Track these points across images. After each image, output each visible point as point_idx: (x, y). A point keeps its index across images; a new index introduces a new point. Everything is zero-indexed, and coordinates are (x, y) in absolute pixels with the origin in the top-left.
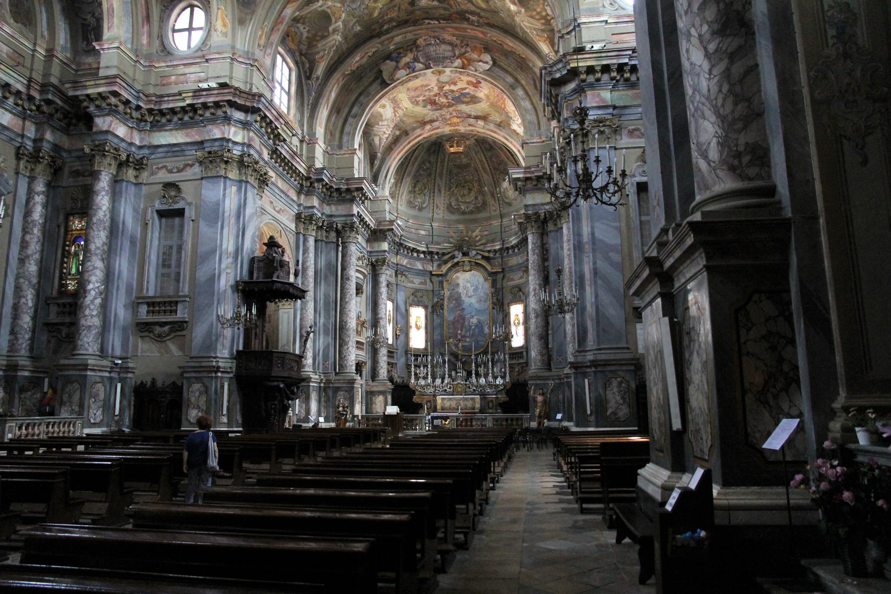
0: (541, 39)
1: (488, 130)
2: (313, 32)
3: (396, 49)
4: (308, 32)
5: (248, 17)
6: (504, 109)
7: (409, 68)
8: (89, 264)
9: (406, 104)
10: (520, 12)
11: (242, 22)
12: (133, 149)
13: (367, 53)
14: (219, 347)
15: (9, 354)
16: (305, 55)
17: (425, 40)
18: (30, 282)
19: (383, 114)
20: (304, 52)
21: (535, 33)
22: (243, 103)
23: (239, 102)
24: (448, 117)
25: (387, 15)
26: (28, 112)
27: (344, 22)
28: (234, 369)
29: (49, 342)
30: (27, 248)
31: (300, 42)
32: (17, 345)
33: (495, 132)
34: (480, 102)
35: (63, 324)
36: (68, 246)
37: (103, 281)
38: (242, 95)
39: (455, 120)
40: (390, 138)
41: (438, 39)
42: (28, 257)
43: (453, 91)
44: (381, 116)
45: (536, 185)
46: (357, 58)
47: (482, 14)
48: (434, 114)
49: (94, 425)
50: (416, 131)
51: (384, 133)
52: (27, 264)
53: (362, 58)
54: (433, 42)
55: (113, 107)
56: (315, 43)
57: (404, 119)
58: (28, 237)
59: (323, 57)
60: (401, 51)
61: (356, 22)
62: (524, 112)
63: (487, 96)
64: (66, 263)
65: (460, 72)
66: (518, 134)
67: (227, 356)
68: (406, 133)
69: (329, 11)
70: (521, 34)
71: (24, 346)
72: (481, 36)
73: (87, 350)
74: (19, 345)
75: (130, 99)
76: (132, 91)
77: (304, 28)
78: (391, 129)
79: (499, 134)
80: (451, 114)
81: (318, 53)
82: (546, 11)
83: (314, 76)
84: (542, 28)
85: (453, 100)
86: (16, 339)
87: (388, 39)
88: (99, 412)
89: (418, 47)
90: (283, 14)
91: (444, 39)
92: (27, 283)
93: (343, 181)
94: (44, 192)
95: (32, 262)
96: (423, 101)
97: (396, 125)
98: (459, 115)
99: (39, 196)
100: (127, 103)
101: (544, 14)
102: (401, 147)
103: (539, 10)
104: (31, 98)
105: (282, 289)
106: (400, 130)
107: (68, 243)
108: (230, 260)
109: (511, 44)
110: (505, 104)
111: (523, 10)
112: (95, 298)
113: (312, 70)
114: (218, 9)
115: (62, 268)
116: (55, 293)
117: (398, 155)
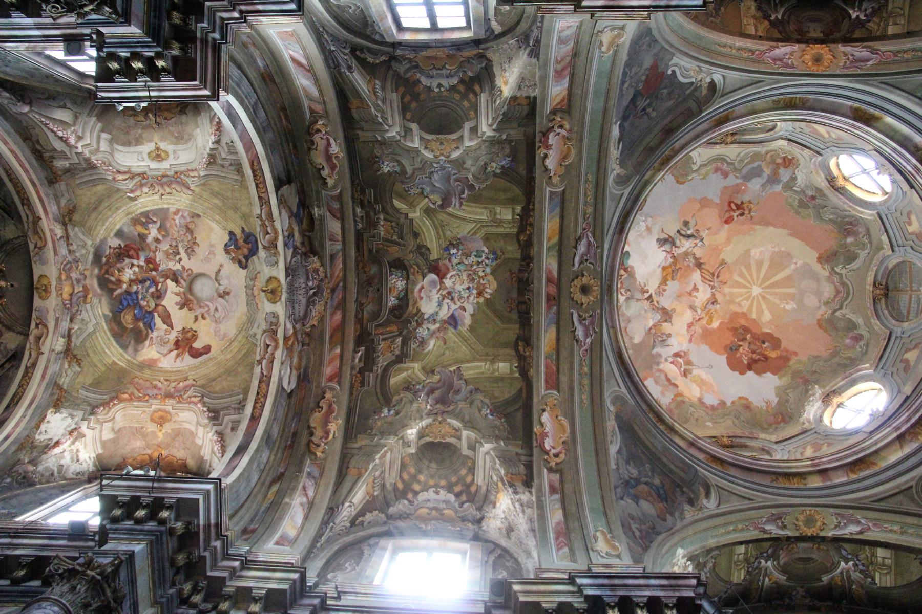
0: (370, 485)
1: (48, 360)
2: (422, 97)
3: (311, 219)
4: (429, 89)
6: (117, 397)
7: (288, 237)
9: (148, 201)
10: (407, 444)
13: (333, 168)
16: (387, 64)
17: (316, 271)
19: (140, 148)
20: (393, 64)
21: (377, 473)
24: (74, 275)
25: (385, 219)
27: (417, 151)
31: (417, 67)
33: (43, 377)
34: (124, 347)
39: (67, 289)
40: (58, 146)
41: (314, 294)
43: (159, 296)
44: (127, 144)
45: (172, 563)
46: (335, 149)
47: (371, 378)
48: (84, 245)
50: (53, 202)
51: (80, 138)
53: (328, 157)
54: (310, 284)
56: (402, 89)
57: (100, 188)
59: (375, 93)
60: (305, 226)
61: (404, 172)
62: (246, 474)
63: (150, 365)
65: (275, 332)
66: (38, 426)
68: (52, 179)
69: (453, 136)
70: (356, 446)
72: (328, 371)
77: (440, 86)
78: (87, 155)
79: (39, 385)
80: (78, 281)
81: (383, 88)
82: (426, 490)
83: (354, 63)
84: (388, 486)
85: (128, 292)
87: (342, 210)
89: (305, 255)
90: (566, 82)
91: (314, 305)
93: (217, 35)
96: (142, 237)
97: (92, 167)
98: (75, 299)
101: (416, 487)
102: (27, 165)
103: (422, 478)
106: (67, 171)
109: (332, 427)
110: (131, 400)
111: (412, 450)
113: (362, 62)
117: (12, 152)
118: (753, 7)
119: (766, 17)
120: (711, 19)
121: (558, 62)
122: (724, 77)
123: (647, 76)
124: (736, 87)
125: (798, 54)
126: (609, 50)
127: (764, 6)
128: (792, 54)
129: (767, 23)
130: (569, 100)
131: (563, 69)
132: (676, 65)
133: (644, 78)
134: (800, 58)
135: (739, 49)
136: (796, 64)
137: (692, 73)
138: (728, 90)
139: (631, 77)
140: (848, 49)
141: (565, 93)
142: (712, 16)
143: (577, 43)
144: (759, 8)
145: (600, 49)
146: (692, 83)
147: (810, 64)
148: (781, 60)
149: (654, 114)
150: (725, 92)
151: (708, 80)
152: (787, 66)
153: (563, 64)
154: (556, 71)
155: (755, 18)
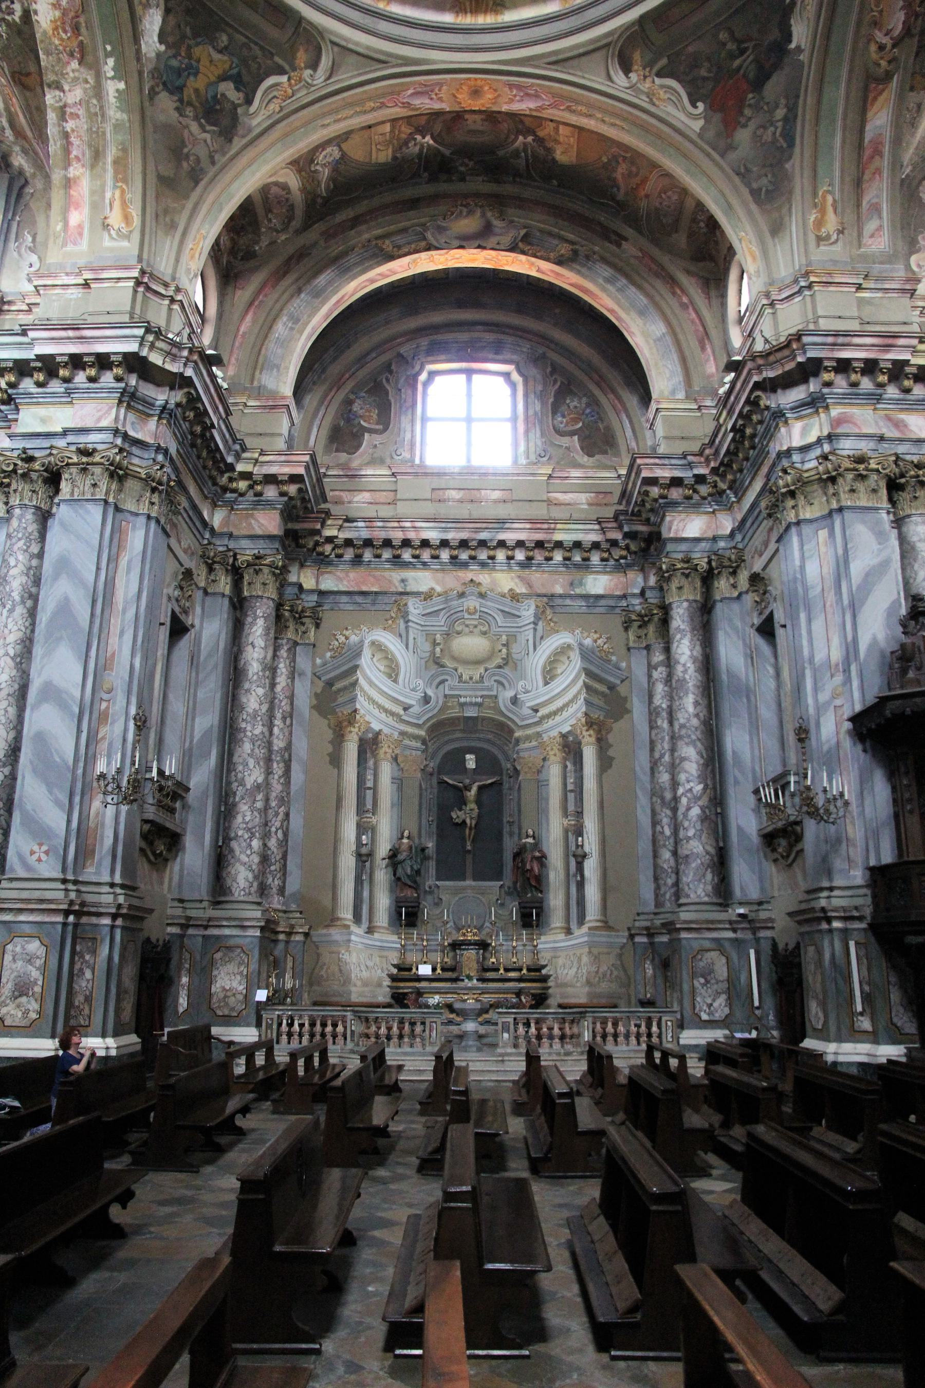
5: (784, 211)
11: (777, 229)
12: (722, 544)
14: (838, 864)
22: (780, 372)
23: (771, 374)
26: (622, 561)
28: (868, 912)
37: (699, 776)
38: (772, 358)
49: (711, 1024)
55: (661, 501)
67: (859, 881)
73: (688, 896)
75: (677, 474)
76: (673, 462)
88: (721, 1001)
90: (869, 134)
100: (676, 482)
104: (614, 543)
105: (908, 711)
108: (839, 678)
112: (689, 809)
114: (740, 240)
118: (558, 152)
119: (540, 141)
120: (628, 155)
121: (878, 171)
122: (609, 78)
123: (741, 113)
124: (584, 59)
125: (500, 100)
126: (824, 197)
127: (542, 151)
128: (511, 101)
129: (541, 134)
130: (865, 100)
131: (872, 157)
132: (695, 117)
133: (747, 112)
134: (499, 96)
135: (590, 116)
136: (507, 89)
137: (662, 94)
138: (599, 55)
139: (772, 123)
140: (437, 106)
141: (870, 114)
142: (625, 158)
143: (858, 205)
144: (549, 151)
145: (834, 200)
146: (659, 75)
147: (486, 88)
148: (527, 95)
149: (723, 36)
150: (604, 52)
151: (634, 76)
152: (519, 87)
153: (872, 167)
154: (881, 155)
155: (557, 142)
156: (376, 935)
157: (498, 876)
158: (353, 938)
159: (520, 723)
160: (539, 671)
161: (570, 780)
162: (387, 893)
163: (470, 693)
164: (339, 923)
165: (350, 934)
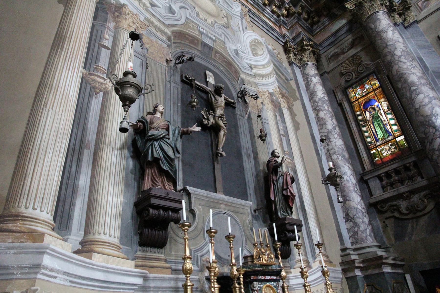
8: (421, 96)
15: (354, 247)
18: (344, 157)
29: (385, 227)
30: (325, 124)
32: (359, 233)
35: (400, 196)
36: (360, 115)
42: (329, 132)
52: (332, 140)
58: (322, 114)
64: (367, 132)
71: (368, 232)
74: (362, 232)
86: (356, 225)
92: (340, 158)
94: (317, 74)
95: (336, 136)
99: (315, 78)
107: (358, 113)
115: (363, 139)
116: (368, 167)
156: (97, 259)
157: (244, 196)
158: (47, 260)
159: (243, 70)
160: (248, 46)
161: (281, 128)
162: (120, 187)
163: (208, 30)
164: (18, 226)
165: (41, 252)
